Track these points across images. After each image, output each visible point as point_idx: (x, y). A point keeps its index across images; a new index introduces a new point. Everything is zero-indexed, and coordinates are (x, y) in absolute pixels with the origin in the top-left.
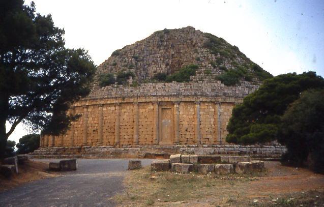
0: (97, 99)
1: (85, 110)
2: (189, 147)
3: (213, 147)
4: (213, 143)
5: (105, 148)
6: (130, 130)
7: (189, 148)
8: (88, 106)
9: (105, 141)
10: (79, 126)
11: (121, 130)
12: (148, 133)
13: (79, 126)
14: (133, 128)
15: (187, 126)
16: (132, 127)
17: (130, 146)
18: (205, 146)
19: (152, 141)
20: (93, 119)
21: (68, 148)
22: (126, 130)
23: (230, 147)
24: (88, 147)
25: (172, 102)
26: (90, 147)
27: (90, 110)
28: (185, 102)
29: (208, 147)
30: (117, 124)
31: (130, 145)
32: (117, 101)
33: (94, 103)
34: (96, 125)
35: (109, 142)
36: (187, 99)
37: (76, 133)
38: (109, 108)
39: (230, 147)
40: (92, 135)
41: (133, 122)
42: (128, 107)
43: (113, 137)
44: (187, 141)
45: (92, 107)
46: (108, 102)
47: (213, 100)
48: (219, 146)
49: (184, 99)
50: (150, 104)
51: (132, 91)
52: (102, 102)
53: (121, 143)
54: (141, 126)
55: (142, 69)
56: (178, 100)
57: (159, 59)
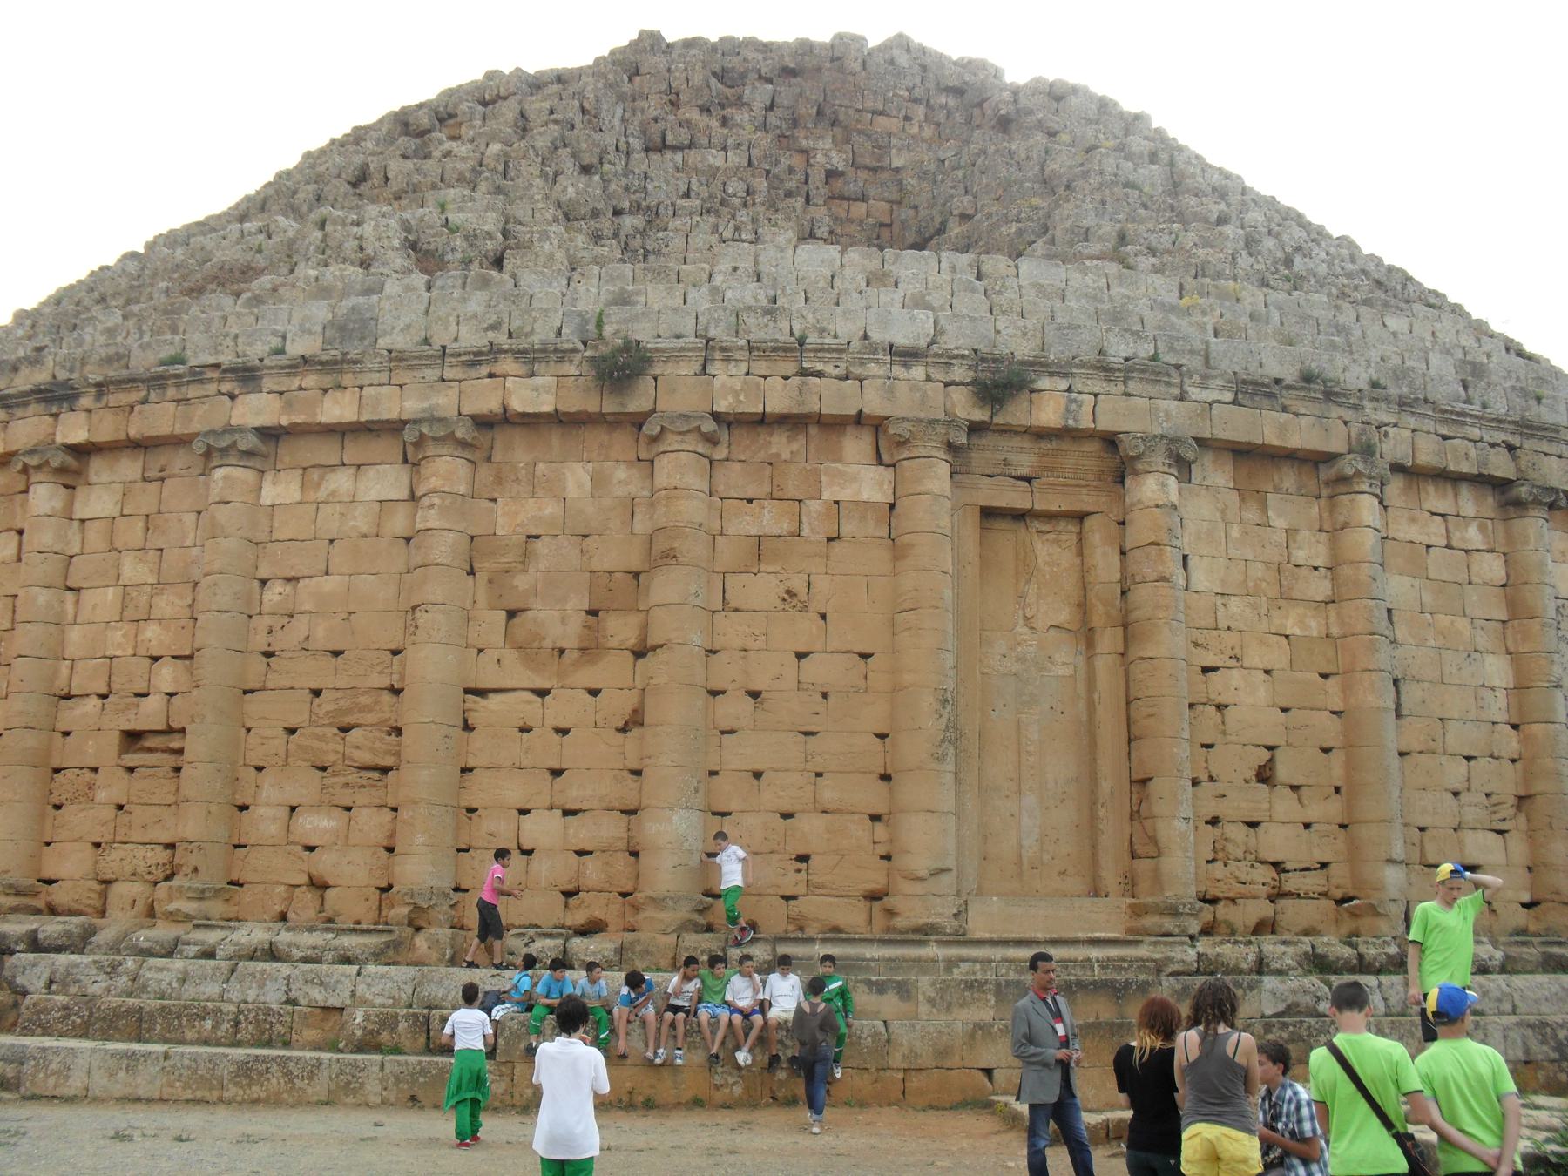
1: (44, 496)
8: (83, 451)
11: (479, 749)
12: (829, 793)
14: (634, 721)
15: (1270, 726)
16: (618, 704)
19: (874, 897)
22: (546, 749)
24: (51, 928)
25: (1110, 441)
26: (79, 943)
27: (98, 501)
28: (1245, 454)
32: (444, 402)
33: (160, 418)
34: (167, 676)
35: (319, 885)
36: (1268, 427)
38: (341, 481)
40: (111, 787)
41: (639, 654)
42: (577, 477)
43: (371, 823)
44: (1276, 895)
45: (129, 467)
46: (338, 409)
47: (1501, 466)
49: (1238, 425)
50: (856, 446)
51: (623, 300)
52: (257, 409)
54: (734, 708)
57: (736, 187)
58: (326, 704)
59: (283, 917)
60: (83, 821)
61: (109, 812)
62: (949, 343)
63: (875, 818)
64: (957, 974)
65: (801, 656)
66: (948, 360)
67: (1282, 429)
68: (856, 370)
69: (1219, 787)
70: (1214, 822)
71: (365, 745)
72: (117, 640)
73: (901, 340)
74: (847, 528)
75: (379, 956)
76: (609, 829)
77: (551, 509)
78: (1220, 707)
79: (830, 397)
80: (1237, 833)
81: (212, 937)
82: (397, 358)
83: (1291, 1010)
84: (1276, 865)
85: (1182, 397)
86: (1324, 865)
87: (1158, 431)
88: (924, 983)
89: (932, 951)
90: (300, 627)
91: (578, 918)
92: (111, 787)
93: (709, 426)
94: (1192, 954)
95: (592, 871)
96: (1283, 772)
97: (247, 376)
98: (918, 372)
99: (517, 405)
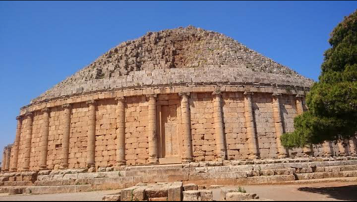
0: (61, 98)
2: (208, 165)
3: (247, 163)
4: (247, 156)
5: (70, 172)
6: (111, 142)
7: (209, 168)
8: (50, 108)
9: (72, 161)
10: (38, 140)
11: (97, 143)
13: (38, 140)
15: (203, 131)
16: (114, 136)
17: (110, 168)
18: (234, 162)
19: (146, 159)
20: (57, 129)
21: (19, 175)
22: (105, 142)
23: (275, 162)
29: (239, 164)
30: (90, 133)
31: (110, 166)
33: (58, 103)
35: (78, 163)
36: (201, 89)
37: (33, 150)
39: (275, 162)
40: (55, 152)
41: (116, 129)
44: (205, 155)
46: (79, 100)
48: (258, 161)
52: (69, 101)
53: (97, 164)
55: (134, 65)
56: (186, 89)
57: (157, 55)
58: (79, 139)
59: (74, 167)
60: (51, 157)
61: (54, 156)
62: (154, 83)
63: (147, 148)
64: (154, 169)
65: (137, 127)
66: (154, 86)
67: (203, 89)
68: (142, 88)
69: (196, 141)
70: (195, 146)
71: (84, 144)
72: (55, 133)
73: (147, 84)
74: (142, 110)
75: (83, 172)
76: (112, 152)
77: (106, 111)
78: (196, 129)
79: (139, 93)
80: (198, 147)
81: (63, 171)
82: (86, 93)
83: (200, 172)
84: (205, 151)
85: (188, 86)
86: (213, 151)
87: (184, 92)
88: (147, 170)
89: (152, 166)
90: (76, 129)
91: (109, 165)
92: (55, 152)
93: (123, 98)
94: (189, 164)
95: (111, 158)
96: (205, 138)
97: (68, 96)
98: (150, 88)
99: (100, 98)
